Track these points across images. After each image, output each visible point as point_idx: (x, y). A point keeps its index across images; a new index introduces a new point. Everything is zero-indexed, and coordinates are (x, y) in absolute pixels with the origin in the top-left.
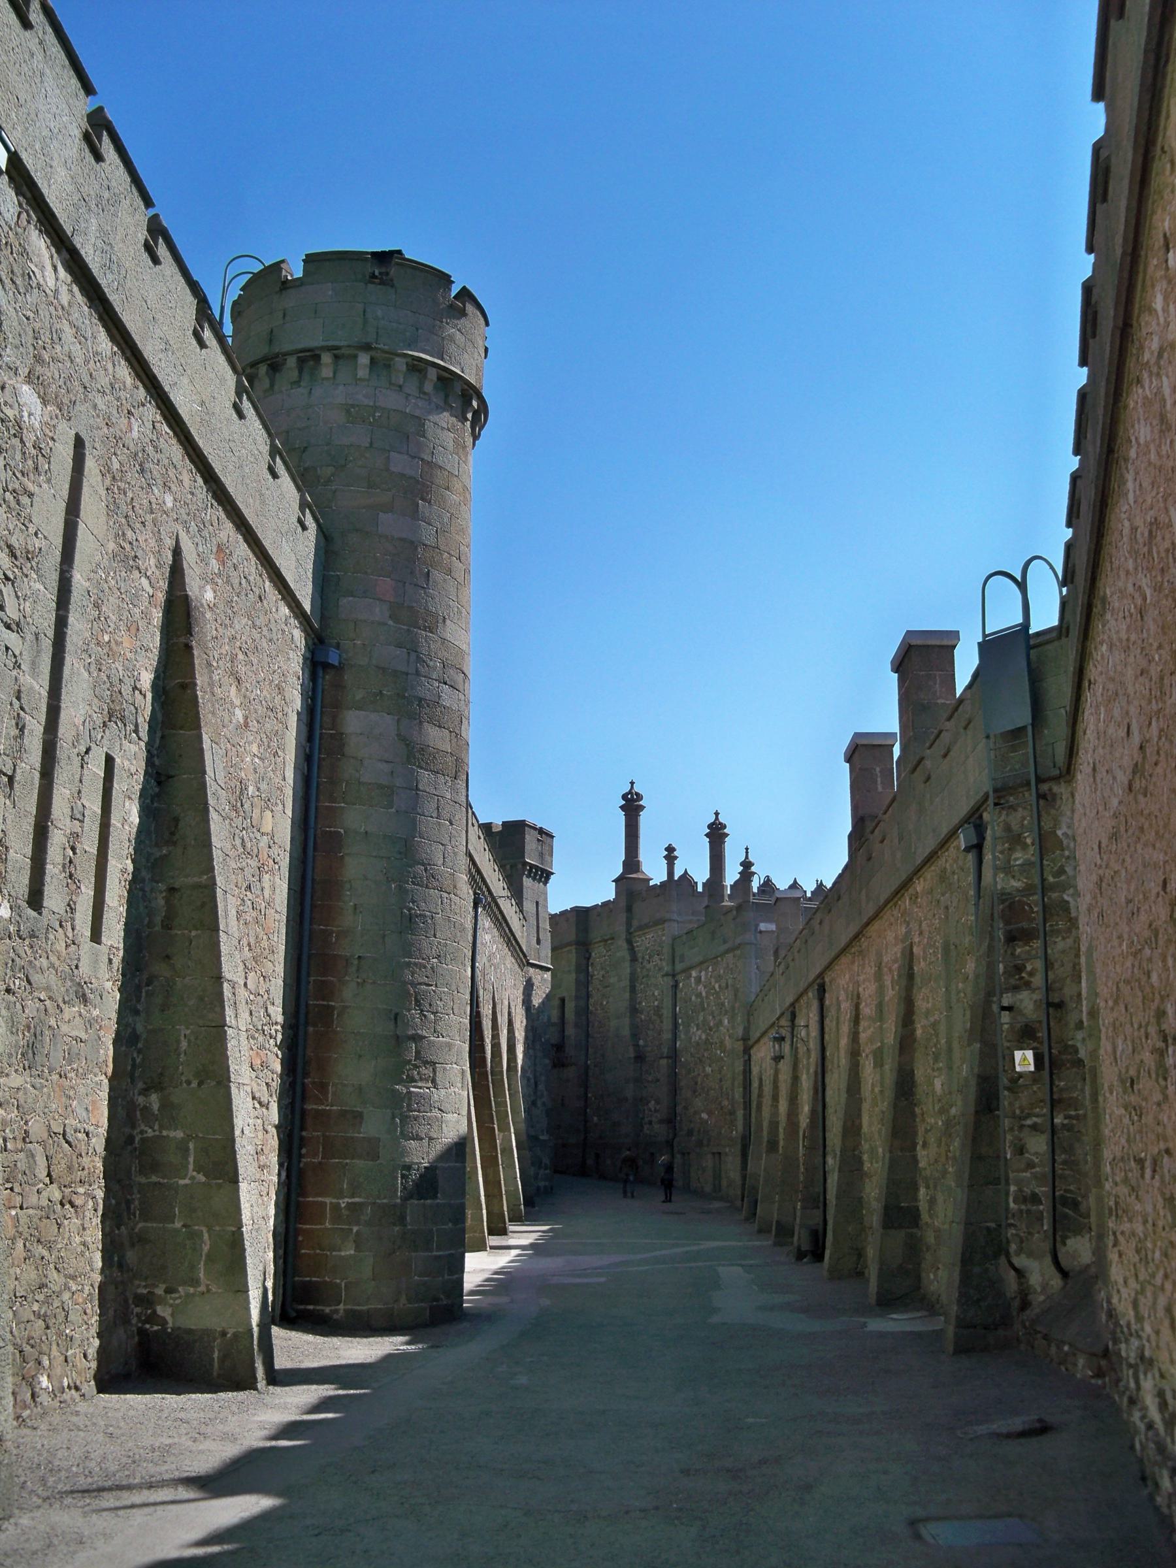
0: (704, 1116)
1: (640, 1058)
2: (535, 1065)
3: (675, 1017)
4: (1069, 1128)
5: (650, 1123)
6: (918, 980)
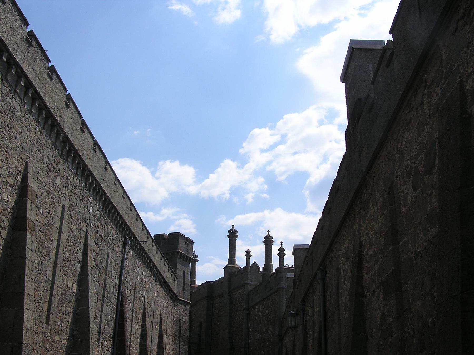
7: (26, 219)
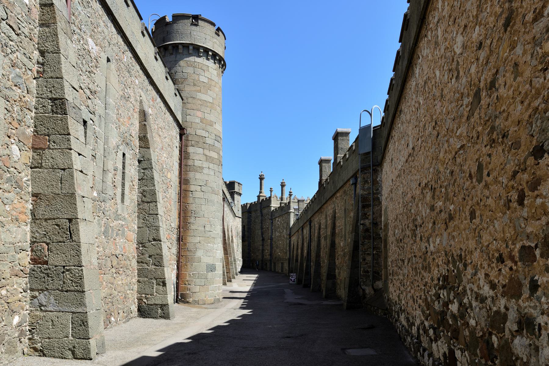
3: (272, 230)
4: (377, 254)
6: (337, 218)
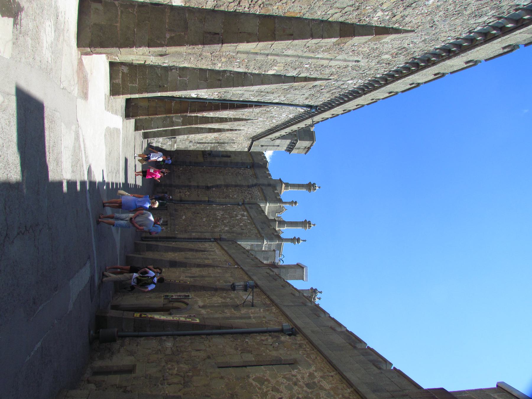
0: (184, 217)
1: (208, 188)
2: (208, 143)
3: (226, 204)
5: (180, 192)
7: (352, 36)
